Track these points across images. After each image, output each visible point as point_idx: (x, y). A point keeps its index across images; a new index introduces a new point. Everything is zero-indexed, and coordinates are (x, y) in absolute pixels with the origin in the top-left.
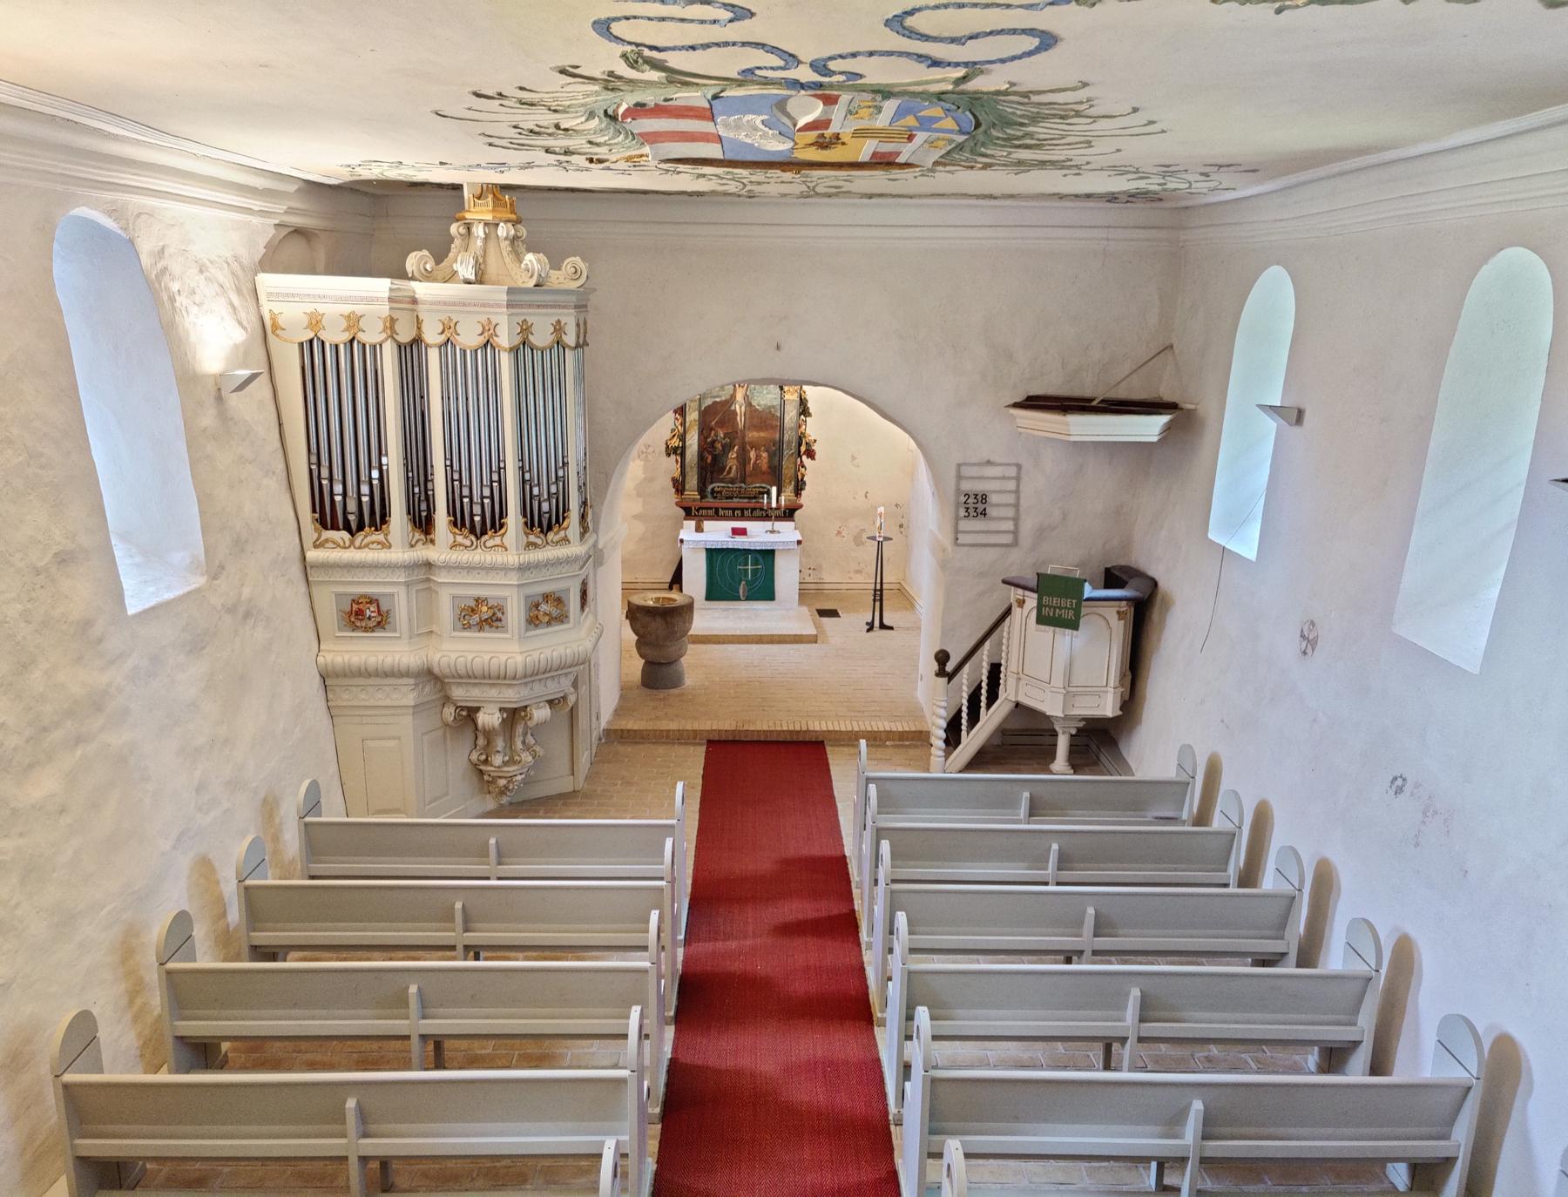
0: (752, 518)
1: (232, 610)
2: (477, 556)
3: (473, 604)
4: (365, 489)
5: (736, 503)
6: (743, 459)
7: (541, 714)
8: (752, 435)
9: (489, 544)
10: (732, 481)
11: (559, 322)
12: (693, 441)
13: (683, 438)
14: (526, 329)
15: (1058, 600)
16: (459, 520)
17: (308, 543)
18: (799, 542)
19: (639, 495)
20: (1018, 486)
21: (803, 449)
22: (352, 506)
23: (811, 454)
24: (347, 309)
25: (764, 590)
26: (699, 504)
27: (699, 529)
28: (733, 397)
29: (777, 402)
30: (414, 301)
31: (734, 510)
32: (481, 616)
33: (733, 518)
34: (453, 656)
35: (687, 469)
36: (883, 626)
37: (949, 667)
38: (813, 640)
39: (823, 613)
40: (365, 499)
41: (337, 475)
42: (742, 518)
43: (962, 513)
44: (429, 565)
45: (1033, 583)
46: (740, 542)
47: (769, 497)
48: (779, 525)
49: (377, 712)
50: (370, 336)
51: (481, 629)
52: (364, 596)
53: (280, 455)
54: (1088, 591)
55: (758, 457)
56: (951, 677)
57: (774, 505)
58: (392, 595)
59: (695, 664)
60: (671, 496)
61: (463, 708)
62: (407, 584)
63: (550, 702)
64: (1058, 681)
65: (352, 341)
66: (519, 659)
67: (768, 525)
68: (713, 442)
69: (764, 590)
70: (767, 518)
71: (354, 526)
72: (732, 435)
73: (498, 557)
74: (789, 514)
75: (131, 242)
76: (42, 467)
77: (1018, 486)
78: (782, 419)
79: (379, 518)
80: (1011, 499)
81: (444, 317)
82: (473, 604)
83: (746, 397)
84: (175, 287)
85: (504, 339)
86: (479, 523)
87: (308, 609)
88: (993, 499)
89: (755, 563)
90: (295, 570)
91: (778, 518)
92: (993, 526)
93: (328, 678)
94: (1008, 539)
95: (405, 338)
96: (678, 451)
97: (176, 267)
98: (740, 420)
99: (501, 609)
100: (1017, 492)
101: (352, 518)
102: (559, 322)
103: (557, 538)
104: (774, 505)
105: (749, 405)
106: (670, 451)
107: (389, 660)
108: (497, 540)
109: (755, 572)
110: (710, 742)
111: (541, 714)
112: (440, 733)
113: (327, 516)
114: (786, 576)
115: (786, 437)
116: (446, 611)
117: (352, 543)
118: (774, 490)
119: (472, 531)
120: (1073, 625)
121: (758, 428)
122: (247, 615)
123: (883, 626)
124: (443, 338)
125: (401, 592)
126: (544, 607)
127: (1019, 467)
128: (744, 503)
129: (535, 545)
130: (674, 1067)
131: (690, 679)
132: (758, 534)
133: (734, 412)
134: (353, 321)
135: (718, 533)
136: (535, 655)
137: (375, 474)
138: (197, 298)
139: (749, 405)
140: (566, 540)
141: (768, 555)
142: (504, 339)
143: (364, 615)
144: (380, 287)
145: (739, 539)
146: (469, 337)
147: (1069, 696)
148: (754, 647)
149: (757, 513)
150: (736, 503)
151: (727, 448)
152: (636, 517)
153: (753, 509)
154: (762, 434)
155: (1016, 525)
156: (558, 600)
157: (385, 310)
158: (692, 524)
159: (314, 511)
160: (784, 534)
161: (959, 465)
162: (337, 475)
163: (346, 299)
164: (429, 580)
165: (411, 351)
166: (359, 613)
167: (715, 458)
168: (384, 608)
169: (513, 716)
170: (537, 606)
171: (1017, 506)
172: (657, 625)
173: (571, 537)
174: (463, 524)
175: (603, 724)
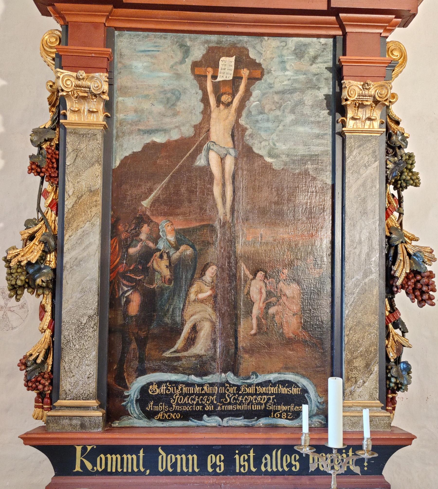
5: (211, 430)
10: (201, 368)
13: (54, 244)
21: (401, 271)
26: (99, 436)
28: (200, 137)
29: (323, 146)
31: (203, 451)
35: (67, 332)
55: (272, 297)
60: (23, 411)
68: (147, 255)
83: (237, 132)
105: (246, 153)
133: (206, 172)
150: (211, 430)
151: (186, 272)
167: (151, 301)
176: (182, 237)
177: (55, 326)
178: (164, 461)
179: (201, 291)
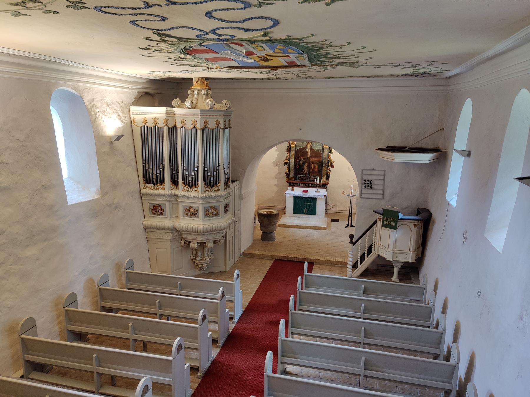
0: (311, 187)
1: (110, 206)
2: (190, 194)
3: (189, 208)
4: (158, 171)
5: (306, 182)
6: (309, 167)
7: (210, 245)
8: (313, 159)
9: (194, 190)
10: (306, 174)
11: (218, 120)
12: (293, 161)
13: (289, 160)
14: (206, 123)
15: (390, 219)
16: (185, 182)
17: (142, 188)
18: (325, 196)
19: (276, 178)
20: (384, 177)
21: (329, 164)
22: (155, 177)
23: (332, 166)
24: (154, 116)
25: (312, 211)
27: (293, 190)
28: (307, 146)
29: (321, 148)
30: (174, 114)
31: (305, 184)
32: (191, 213)
33: (305, 187)
34: (182, 224)
36: (352, 226)
37: (354, 240)
38: (325, 229)
39: (333, 220)
40: (158, 174)
41: (151, 167)
42: (308, 187)
43: (363, 187)
44: (177, 196)
45: (382, 213)
46: (305, 195)
47: (317, 181)
48: (320, 190)
49: (158, 240)
50: (161, 124)
51: (191, 217)
52: (157, 204)
53: (135, 159)
54: (401, 216)
55: (314, 167)
56: (354, 244)
57: (318, 183)
58: (165, 204)
59: (278, 233)
60: (285, 179)
61: (187, 241)
62: (170, 201)
63: (215, 242)
64: (391, 248)
65: (155, 126)
66: (201, 227)
67: (316, 189)
68: (300, 161)
69: (312, 211)
70: (316, 187)
71: (155, 183)
72: (306, 159)
73: (196, 194)
74: (324, 186)
75: (81, 97)
76: (41, 161)
77: (384, 177)
78: (323, 154)
79: (161, 181)
80: (382, 183)
81: (182, 119)
82: (189, 208)
83: (311, 146)
84: (97, 110)
85: (199, 126)
86: (191, 184)
87: (141, 207)
88: (375, 182)
89: (310, 202)
90: (137, 195)
91: (320, 187)
92: (375, 192)
93: (146, 229)
94: (380, 197)
95: (171, 125)
96: (287, 164)
97: (98, 105)
98: (309, 154)
99: (197, 211)
100: (384, 180)
101: (154, 180)
102: (218, 120)
103: (215, 189)
104: (318, 183)
105: (312, 149)
106: (285, 164)
107: (163, 224)
108: (196, 189)
109: (310, 205)
110: (276, 259)
111: (210, 245)
112: (181, 248)
113: (148, 179)
114: (320, 206)
115: (324, 160)
116: (181, 210)
117: (154, 187)
118: (318, 178)
119: (189, 186)
120: (395, 228)
121: (314, 157)
122: (116, 208)
123: (352, 226)
124: (181, 126)
125: (168, 204)
126: (211, 211)
127: (385, 171)
128: (309, 182)
129: (208, 191)
130: (215, 362)
131: (277, 239)
132: (312, 192)
134: (156, 120)
135: (298, 191)
136: (207, 226)
137: (161, 167)
138: (106, 114)
139: (312, 149)
140: (219, 190)
141: (314, 200)
142: (199, 126)
143: (157, 210)
144: (163, 110)
145: (305, 194)
146: (189, 125)
147: (395, 253)
148: (304, 230)
149: (313, 185)
150: (306, 182)
151: (304, 163)
152: (275, 185)
153: (312, 184)
154: (316, 159)
155: (383, 192)
156: (216, 209)
157: (164, 116)
158: (290, 188)
159: (144, 178)
160: (322, 192)
161: (362, 170)
162: (151, 167)
163: (154, 114)
164: (177, 200)
165: (173, 130)
166: (155, 210)
167: (299, 166)
168: (163, 208)
169: (202, 245)
170: (208, 210)
171: (384, 185)
172: (265, 220)
173: (220, 189)
174: (187, 184)
175: (242, 251)
176: (304, 159)
177: (289, 169)
178: (301, 185)
179: (306, 166)
